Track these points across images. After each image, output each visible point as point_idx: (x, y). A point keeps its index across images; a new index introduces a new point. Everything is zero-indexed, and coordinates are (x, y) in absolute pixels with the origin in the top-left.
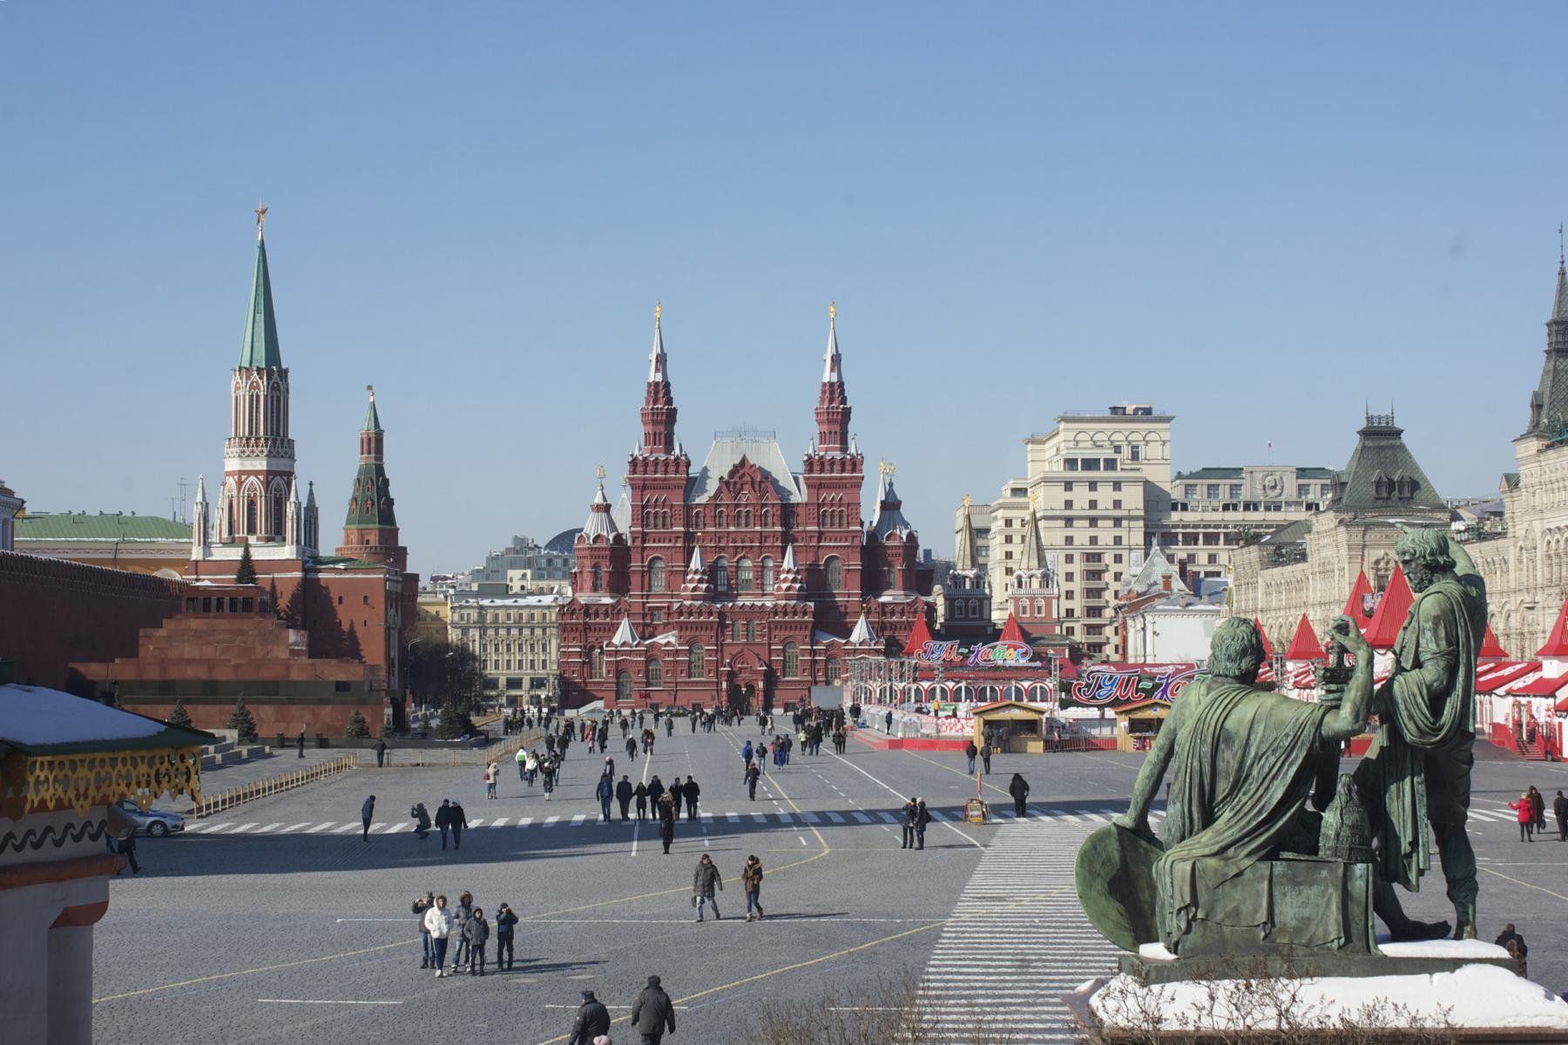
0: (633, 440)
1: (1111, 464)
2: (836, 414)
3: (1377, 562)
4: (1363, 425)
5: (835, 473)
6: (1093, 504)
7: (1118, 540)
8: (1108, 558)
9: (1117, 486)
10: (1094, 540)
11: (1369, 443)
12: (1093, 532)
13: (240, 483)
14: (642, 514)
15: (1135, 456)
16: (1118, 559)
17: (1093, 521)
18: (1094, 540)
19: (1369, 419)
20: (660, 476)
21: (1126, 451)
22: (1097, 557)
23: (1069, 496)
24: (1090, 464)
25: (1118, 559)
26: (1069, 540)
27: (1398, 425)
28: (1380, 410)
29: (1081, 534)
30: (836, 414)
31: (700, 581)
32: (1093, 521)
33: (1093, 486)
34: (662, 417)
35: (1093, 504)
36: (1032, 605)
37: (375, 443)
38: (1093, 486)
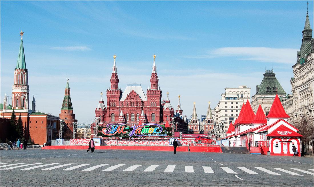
0: (108, 86)
1: (236, 98)
3: (266, 108)
4: (265, 73)
5: (155, 93)
6: (232, 107)
10: (232, 115)
11: (266, 78)
12: (232, 113)
13: (15, 95)
14: (109, 103)
17: (232, 111)
20: (115, 93)
21: (240, 96)
23: (226, 105)
24: (231, 98)
26: (226, 115)
27: (274, 73)
28: (269, 69)
29: (229, 113)
30: (155, 80)
31: (122, 119)
32: (232, 111)
33: (232, 103)
34: (115, 81)
35: (232, 107)
36: (209, 127)
37: (68, 91)
38: (232, 103)
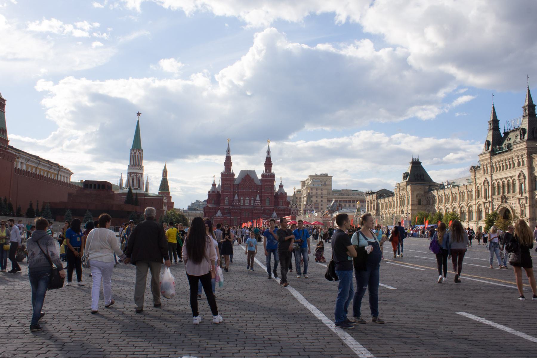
0: (222, 169)
2: (268, 164)
4: (411, 161)
5: (269, 177)
7: (322, 201)
8: (320, 205)
9: (322, 189)
10: (317, 201)
15: (325, 183)
16: (322, 205)
18: (317, 201)
19: (413, 159)
22: (318, 204)
25: (322, 205)
27: (420, 161)
28: (415, 157)
30: (268, 164)
